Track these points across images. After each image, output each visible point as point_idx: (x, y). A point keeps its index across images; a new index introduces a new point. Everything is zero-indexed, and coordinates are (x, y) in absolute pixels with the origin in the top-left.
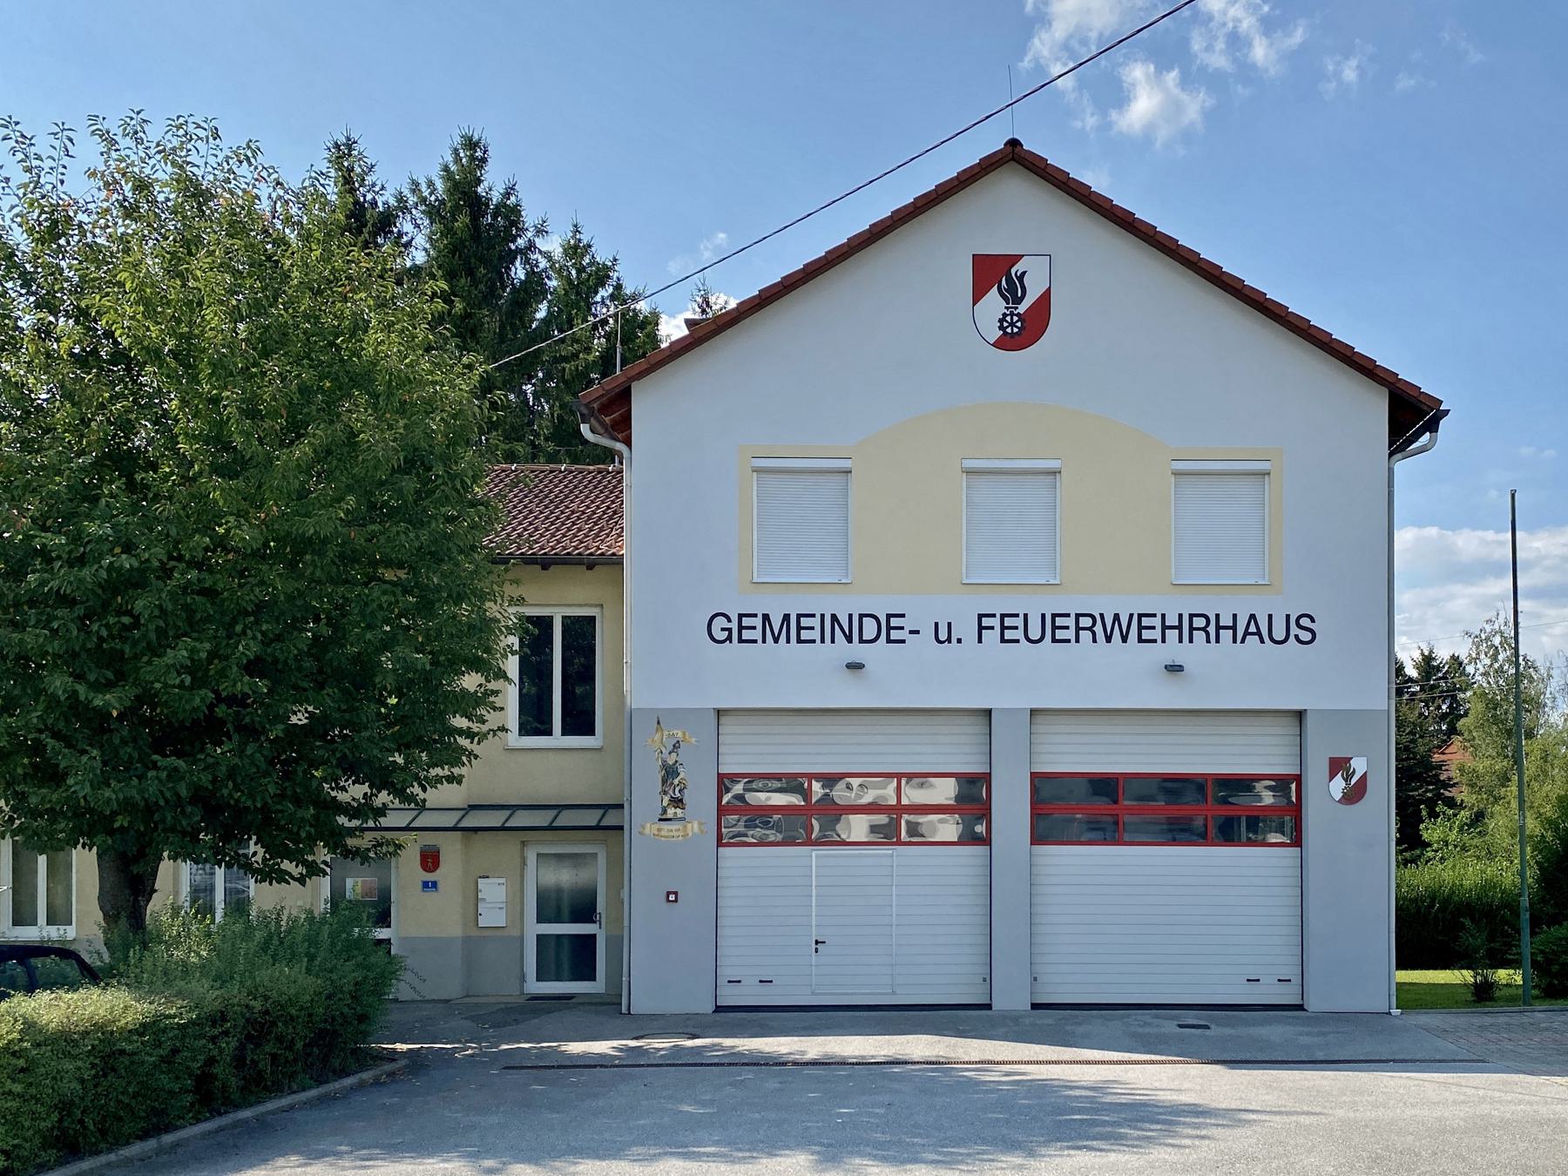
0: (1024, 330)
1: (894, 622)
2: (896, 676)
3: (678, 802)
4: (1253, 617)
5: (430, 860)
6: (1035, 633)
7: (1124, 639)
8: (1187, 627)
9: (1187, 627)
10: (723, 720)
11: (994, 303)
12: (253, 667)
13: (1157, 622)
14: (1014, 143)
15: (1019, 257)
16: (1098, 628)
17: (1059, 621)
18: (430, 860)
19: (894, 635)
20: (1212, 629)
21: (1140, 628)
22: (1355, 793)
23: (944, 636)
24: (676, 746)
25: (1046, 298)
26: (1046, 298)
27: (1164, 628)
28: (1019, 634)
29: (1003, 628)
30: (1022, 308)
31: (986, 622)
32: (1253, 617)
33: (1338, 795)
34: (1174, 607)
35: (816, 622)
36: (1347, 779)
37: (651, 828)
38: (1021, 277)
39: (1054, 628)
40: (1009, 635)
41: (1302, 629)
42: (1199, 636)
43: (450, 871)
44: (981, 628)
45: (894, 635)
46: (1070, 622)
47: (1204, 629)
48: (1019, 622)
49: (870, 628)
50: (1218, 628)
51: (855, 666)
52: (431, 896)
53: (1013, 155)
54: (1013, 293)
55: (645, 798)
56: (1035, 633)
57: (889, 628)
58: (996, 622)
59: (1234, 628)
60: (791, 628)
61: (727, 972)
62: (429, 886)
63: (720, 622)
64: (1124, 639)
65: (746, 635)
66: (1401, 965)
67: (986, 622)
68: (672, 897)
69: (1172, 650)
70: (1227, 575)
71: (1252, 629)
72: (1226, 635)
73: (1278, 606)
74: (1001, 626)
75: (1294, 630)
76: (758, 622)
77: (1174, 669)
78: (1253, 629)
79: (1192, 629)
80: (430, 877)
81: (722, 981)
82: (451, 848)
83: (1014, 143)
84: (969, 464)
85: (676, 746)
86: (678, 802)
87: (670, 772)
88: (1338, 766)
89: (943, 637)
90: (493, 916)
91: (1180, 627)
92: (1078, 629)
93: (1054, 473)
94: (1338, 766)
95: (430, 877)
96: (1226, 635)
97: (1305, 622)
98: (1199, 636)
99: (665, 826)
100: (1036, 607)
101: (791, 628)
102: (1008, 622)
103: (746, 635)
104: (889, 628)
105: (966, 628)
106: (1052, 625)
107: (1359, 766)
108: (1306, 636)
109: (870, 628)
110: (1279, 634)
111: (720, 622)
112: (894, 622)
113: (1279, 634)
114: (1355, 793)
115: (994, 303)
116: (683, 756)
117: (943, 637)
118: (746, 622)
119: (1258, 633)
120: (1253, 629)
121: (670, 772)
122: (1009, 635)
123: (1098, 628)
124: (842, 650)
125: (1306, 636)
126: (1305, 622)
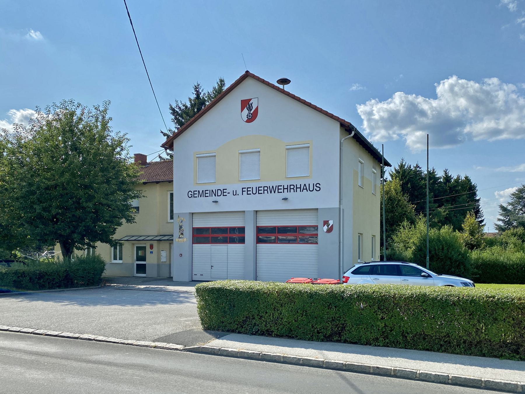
0: (251, 118)
1: (225, 191)
2: (227, 203)
3: (182, 234)
4: (305, 185)
5: (152, 247)
6: (254, 192)
7: (275, 192)
8: (289, 188)
9: (289, 188)
10: (258, 213)
11: (246, 111)
12: (58, 207)
13: (282, 187)
14: (247, 72)
15: (251, 99)
16: (269, 190)
17: (260, 189)
18: (152, 247)
19: (225, 194)
20: (295, 189)
21: (278, 189)
22: (330, 230)
23: (235, 194)
24: (182, 221)
25: (257, 109)
26: (257, 109)
27: (284, 189)
28: (251, 192)
29: (248, 191)
30: (252, 112)
31: (244, 190)
32: (305, 185)
33: (325, 230)
34: (286, 183)
35: (208, 192)
36: (328, 226)
37: (177, 240)
38: (251, 104)
39: (259, 190)
40: (249, 193)
41: (317, 187)
42: (292, 190)
43: (155, 250)
44: (243, 191)
45: (225, 194)
46: (262, 189)
47: (293, 189)
48: (251, 189)
49: (219, 192)
50: (297, 188)
51: (216, 202)
52: (152, 255)
53: (247, 75)
54: (250, 109)
55: (176, 234)
56: (254, 192)
57: (223, 192)
58: (246, 190)
59: (300, 188)
60: (203, 194)
61: (194, 273)
62: (151, 252)
63: (190, 193)
64: (275, 192)
65: (195, 196)
66: (145, 265)
67: (244, 190)
68: (181, 255)
69: (286, 194)
70: (298, 174)
71: (305, 188)
72: (298, 190)
73: (310, 182)
74: (247, 191)
75: (315, 187)
76: (197, 192)
77: (285, 199)
78: (305, 188)
79: (290, 189)
80: (151, 251)
81: (193, 274)
82: (155, 244)
83: (247, 72)
84: (240, 152)
85: (182, 221)
86: (182, 234)
87: (181, 227)
88: (326, 223)
89: (235, 194)
90: (163, 259)
91: (287, 189)
92: (264, 190)
93: (215, 156)
94: (326, 223)
95: (151, 251)
96: (298, 190)
97: (318, 185)
98: (292, 190)
99: (180, 239)
100: (254, 185)
101: (203, 194)
102: (249, 189)
103: (195, 196)
104: (223, 192)
105: (239, 192)
106: (258, 189)
107: (331, 223)
108: (318, 189)
109: (219, 192)
110: (311, 189)
111: (190, 193)
112: (225, 191)
113: (311, 189)
114: (330, 230)
115: (246, 111)
116: (183, 223)
117: (235, 194)
118: (195, 193)
119: (306, 189)
120: (305, 188)
121: (181, 227)
122: (249, 193)
123: (269, 190)
124: (214, 198)
125: (318, 189)
126: (318, 185)
